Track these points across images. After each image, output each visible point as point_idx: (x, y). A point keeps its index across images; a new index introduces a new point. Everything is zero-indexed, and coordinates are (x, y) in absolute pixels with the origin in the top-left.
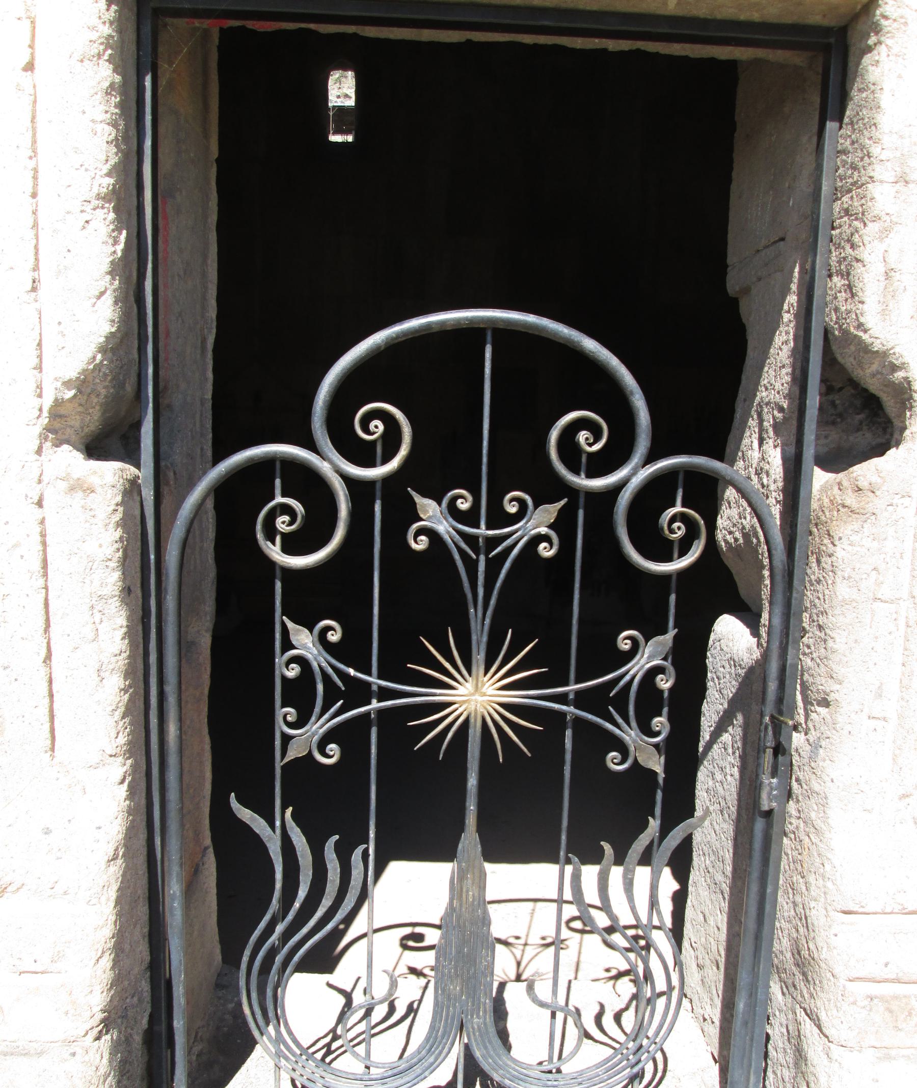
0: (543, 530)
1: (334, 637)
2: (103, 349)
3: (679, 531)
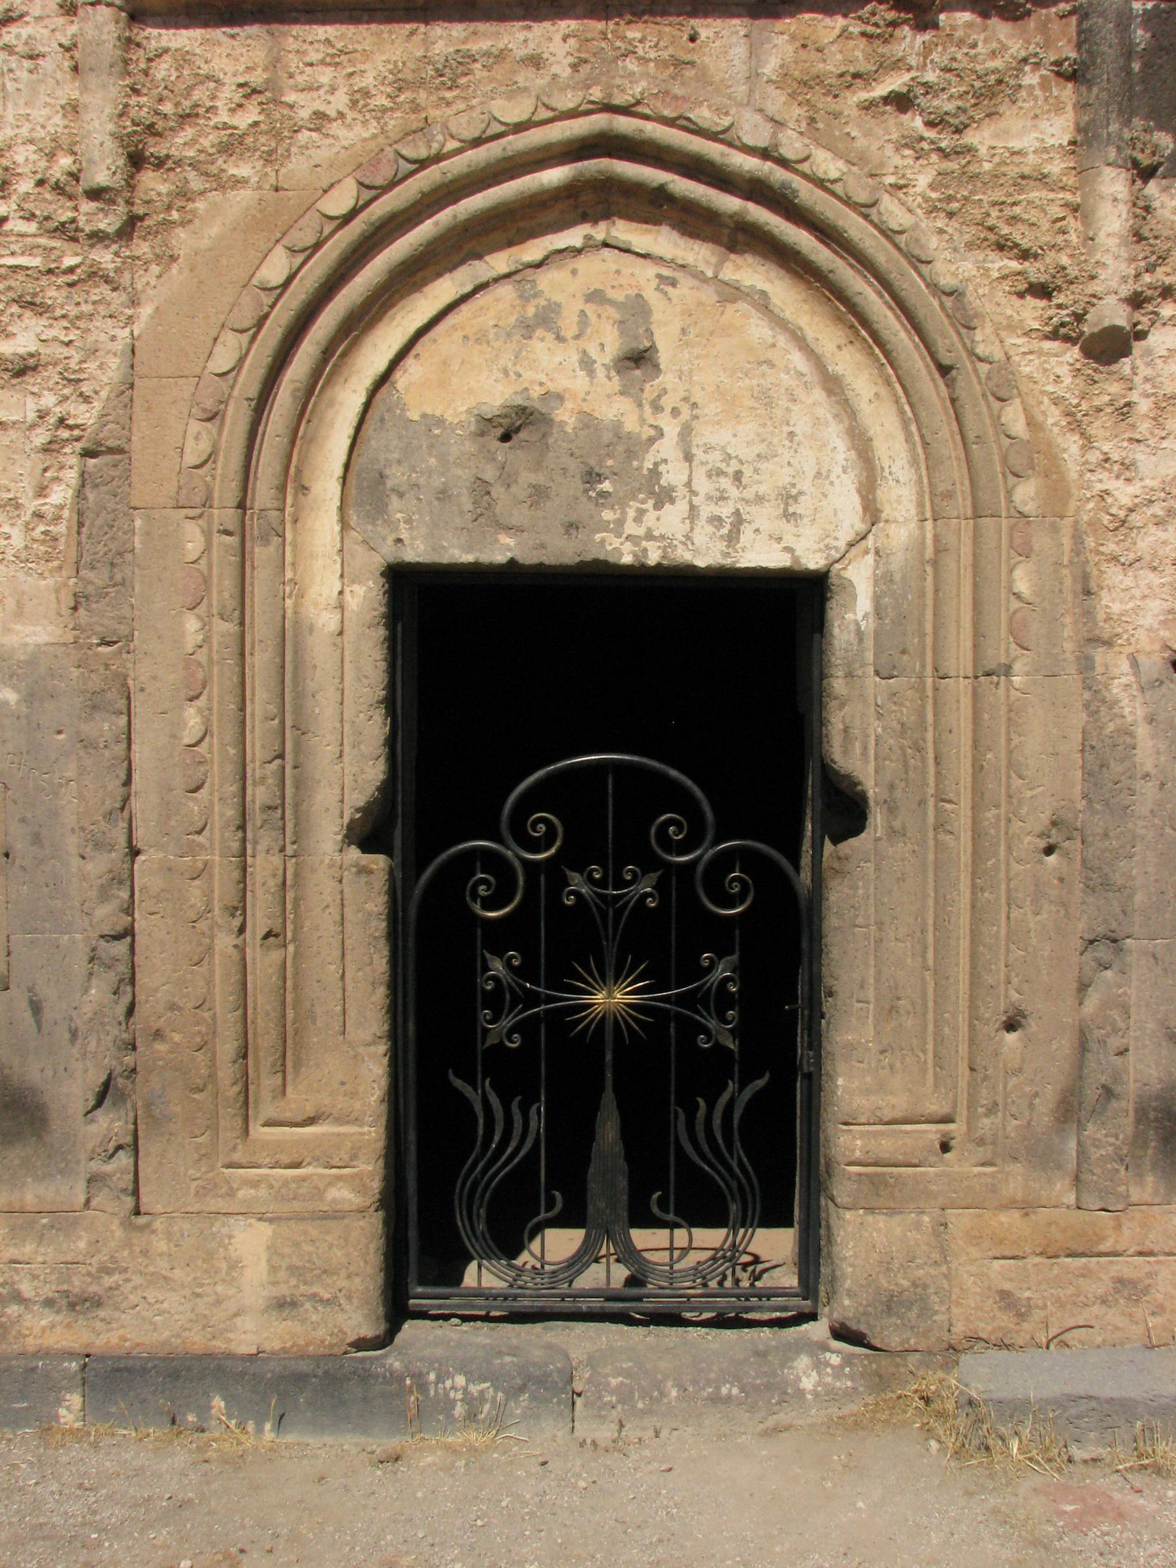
0: (649, 889)
1: (516, 963)
2: (378, 789)
3: (736, 889)
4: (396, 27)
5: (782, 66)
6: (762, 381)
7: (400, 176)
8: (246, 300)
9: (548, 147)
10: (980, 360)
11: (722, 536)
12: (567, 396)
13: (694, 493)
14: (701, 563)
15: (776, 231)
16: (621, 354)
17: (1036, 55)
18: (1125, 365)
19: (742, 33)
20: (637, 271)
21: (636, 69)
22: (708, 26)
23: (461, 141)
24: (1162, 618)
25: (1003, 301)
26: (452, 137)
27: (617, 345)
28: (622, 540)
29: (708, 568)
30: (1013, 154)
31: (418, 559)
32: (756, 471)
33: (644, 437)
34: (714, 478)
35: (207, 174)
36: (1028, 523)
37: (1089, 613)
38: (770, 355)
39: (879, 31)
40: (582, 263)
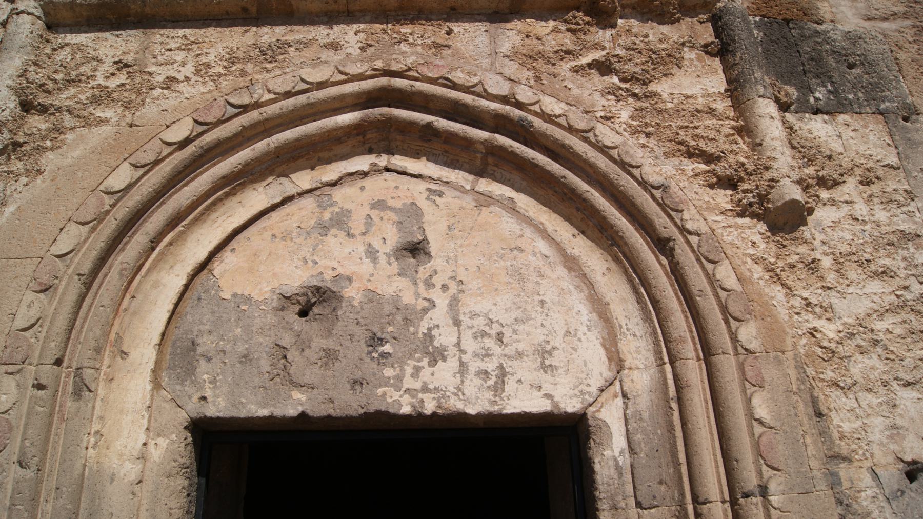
4: (235, 29)
5: (513, 48)
6: (515, 262)
7: (227, 116)
8: (93, 201)
9: (343, 97)
10: (690, 233)
11: (489, 387)
12: (355, 278)
13: (462, 351)
14: (472, 410)
15: (518, 151)
16: (399, 245)
17: (690, 42)
18: (805, 232)
19: (483, 30)
20: (411, 187)
21: (408, 50)
22: (459, 26)
23: (275, 94)
24: (887, 433)
25: (700, 191)
26: (269, 91)
27: (396, 238)
28: (402, 393)
29: (479, 416)
30: (688, 97)
31: (218, 414)
32: (515, 332)
33: (419, 308)
34: (479, 339)
35: (79, 117)
36: (756, 358)
37: (824, 433)
38: (519, 243)
39: (580, 27)
40: (368, 182)
